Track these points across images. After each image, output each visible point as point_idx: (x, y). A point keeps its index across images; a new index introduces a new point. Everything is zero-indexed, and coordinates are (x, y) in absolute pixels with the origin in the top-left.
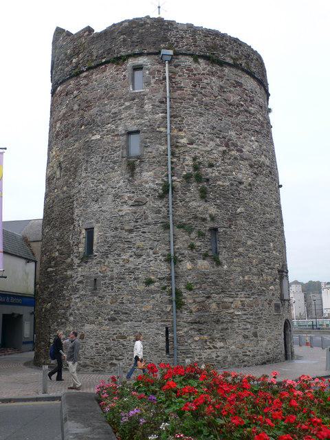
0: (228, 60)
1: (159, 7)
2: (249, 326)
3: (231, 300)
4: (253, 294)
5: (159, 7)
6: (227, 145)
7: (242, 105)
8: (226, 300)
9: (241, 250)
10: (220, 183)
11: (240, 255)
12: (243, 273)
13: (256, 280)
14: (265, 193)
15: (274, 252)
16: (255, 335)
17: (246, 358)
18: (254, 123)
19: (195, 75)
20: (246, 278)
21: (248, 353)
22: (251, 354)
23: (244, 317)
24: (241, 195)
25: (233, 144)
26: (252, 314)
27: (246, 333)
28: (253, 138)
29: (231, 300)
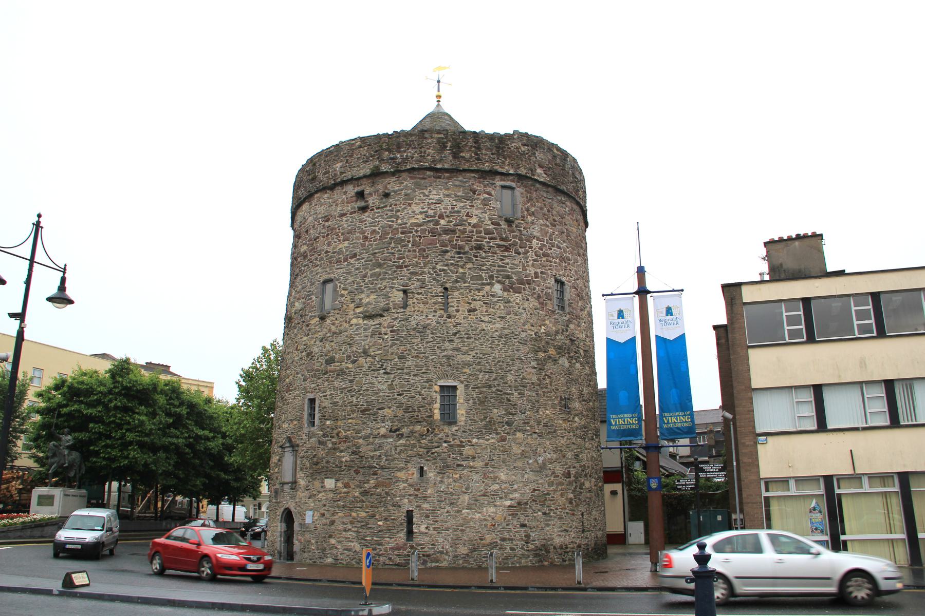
1: (439, 82)
5: (439, 82)
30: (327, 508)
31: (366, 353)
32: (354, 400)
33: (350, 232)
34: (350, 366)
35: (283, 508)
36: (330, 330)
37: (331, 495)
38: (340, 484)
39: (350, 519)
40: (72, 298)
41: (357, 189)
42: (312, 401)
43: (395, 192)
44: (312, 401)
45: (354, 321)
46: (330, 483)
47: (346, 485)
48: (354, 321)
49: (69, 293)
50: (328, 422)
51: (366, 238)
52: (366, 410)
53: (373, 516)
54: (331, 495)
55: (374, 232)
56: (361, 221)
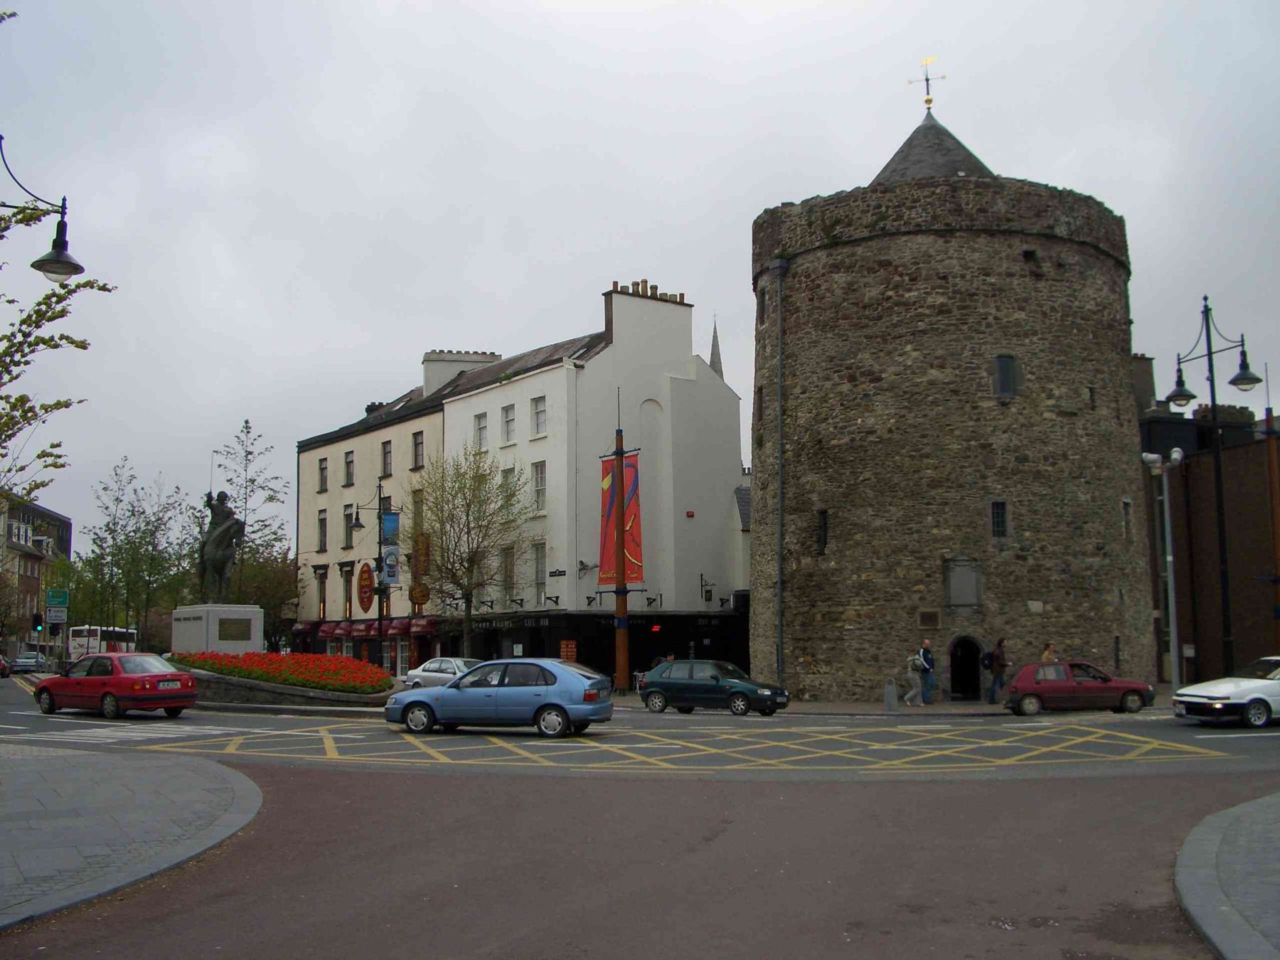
0: (858, 235)
1: (927, 80)
2: (867, 646)
3: (841, 609)
4: (875, 600)
6: (852, 379)
7: (890, 298)
8: (833, 609)
9: (858, 537)
10: (834, 442)
11: (858, 544)
12: (858, 570)
13: (880, 580)
14: (924, 436)
15: (935, 531)
16: (875, 658)
17: (858, 690)
18: (921, 317)
19: (813, 281)
20: (864, 577)
21: (861, 683)
22: (867, 684)
23: (858, 633)
24: (870, 452)
25: (863, 374)
26: (872, 629)
27: (861, 656)
28: (909, 348)
29: (841, 609)
30: (1035, 635)
31: (1065, 456)
32: (1058, 509)
33: (1026, 300)
34: (1050, 468)
35: (949, 641)
36: (1017, 420)
37: (1038, 620)
38: (1049, 607)
39: (1063, 646)
40: (1194, 393)
41: (1025, 247)
42: (999, 507)
43: (1070, 265)
44: (999, 507)
45: (1046, 415)
46: (1036, 606)
47: (1058, 609)
48: (1046, 415)
49: (1189, 386)
50: (1027, 534)
51: (1045, 314)
52: (1072, 522)
53: (1088, 643)
54: (1038, 620)
55: (1053, 309)
56: (1037, 290)
